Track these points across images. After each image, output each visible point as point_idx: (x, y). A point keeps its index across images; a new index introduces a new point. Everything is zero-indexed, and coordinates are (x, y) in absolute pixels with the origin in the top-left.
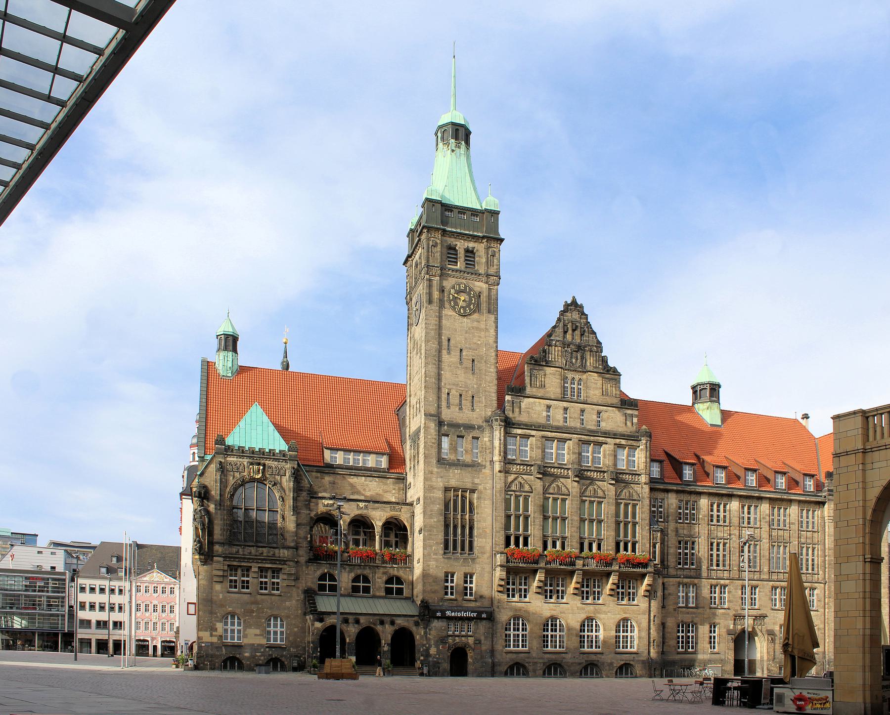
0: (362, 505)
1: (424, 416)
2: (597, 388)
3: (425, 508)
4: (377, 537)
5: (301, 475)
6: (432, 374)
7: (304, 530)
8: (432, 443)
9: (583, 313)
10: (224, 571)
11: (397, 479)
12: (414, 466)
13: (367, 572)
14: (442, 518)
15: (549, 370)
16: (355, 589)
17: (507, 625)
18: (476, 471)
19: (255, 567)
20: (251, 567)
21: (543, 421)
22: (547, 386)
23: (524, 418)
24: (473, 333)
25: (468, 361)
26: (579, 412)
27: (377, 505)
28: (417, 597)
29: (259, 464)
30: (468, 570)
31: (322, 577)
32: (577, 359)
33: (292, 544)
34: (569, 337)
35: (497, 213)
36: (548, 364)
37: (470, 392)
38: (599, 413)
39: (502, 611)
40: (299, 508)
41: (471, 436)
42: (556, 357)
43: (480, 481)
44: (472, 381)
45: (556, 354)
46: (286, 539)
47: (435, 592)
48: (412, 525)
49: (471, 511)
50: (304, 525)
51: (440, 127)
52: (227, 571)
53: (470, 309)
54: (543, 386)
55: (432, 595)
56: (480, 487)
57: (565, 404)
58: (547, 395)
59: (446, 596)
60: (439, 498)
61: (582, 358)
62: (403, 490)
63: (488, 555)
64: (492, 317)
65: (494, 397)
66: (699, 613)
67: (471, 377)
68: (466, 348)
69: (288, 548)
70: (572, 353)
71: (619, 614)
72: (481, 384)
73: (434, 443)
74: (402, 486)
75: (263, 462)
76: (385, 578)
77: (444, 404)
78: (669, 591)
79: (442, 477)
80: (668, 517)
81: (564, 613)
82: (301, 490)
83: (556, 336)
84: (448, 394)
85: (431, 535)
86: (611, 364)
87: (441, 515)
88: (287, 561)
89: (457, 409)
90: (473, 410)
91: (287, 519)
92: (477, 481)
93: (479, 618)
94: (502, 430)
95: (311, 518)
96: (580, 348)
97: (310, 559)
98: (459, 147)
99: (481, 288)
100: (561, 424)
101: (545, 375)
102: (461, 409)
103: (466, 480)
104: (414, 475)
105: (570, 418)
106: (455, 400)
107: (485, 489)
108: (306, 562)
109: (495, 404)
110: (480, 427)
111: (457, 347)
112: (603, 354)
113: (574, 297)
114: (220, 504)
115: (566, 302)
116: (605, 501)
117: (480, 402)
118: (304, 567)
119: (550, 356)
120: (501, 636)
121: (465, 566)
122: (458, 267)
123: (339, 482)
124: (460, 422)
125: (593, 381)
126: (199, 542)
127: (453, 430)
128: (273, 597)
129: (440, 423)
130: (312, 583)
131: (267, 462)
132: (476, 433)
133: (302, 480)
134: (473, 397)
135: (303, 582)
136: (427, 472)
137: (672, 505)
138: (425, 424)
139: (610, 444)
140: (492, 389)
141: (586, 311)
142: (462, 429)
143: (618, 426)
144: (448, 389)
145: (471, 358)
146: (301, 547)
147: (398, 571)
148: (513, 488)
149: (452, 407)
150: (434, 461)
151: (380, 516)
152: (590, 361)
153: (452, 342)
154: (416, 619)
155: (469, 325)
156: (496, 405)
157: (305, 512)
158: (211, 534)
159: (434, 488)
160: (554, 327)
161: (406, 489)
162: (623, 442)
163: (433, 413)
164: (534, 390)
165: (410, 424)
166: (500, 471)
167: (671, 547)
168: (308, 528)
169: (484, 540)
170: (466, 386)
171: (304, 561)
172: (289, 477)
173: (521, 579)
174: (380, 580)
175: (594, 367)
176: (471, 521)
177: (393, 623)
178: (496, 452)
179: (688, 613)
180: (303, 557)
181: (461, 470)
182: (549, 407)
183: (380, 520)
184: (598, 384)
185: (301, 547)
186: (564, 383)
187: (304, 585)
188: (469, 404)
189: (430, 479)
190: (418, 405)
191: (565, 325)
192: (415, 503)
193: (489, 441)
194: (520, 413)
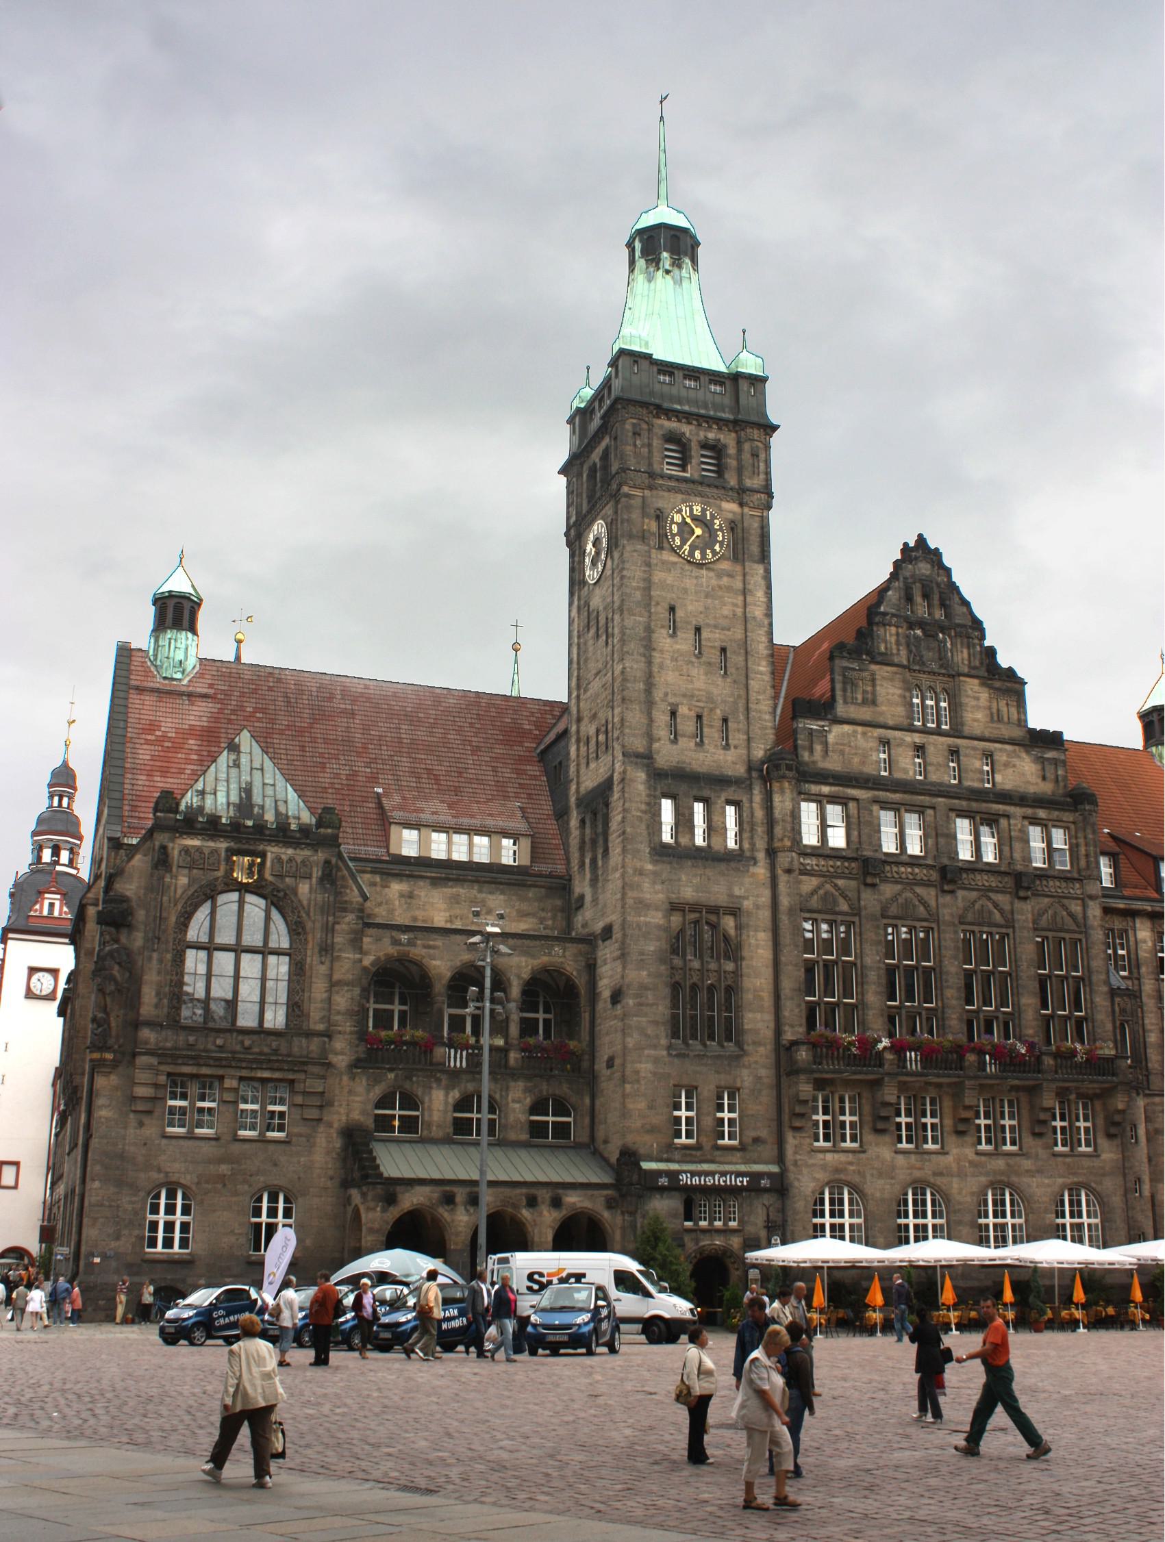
1: (620, 757)
2: (978, 708)
5: (343, 877)
6: (639, 674)
7: (349, 995)
8: (642, 811)
10: (156, 1086)
11: (550, 888)
12: (594, 861)
15: (881, 671)
16: (462, 1127)
17: (815, 1204)
19: (232, 1077)
20: (221, 1078)
22: (880, 699)
23: (833, 764)
24: (722, 597)
28: (606, 1142)
30: (724, 1079)
33: (321, 1027)
35: (763, 380)
37: (718, 711)
40: (337, 947)
41: (723, 799)
44: (723, 689)
46: (309, 1015)
47: (652, 1130)
50: (347, 984)
51: (640, 232)
52: (165, 1086)
53: (714, 553)
55: (647, 1138)
56: (747, 904)
57: (917, 738)
58: (881, 720)
59: (676, 1141)
67: (720, 681)
68: (708, 625)
69: (309, 1034)
73: (645, 812)
80: (1138, 967)
81: (941, 1174)
82: (345, 910)
85: (641, 1004)
86: (1004, 661)
89: (692, 744)
92: (737, 891)
95: (365, 969)
97: (358, 1060)
98: (680, 267)
99: (734, 513)
101: (873, 680)
103: (716, 888)
108: (356, 1064)
111: (688, 623)
113: (920, 536)
114: (159, 939)
115: (906, 544)
118: (345, 1078)
120: (804, 1228)
122: (688, 475)
123: (423, 894)
128: (271, 1147)
130: (363, 1112)
132: (730, 793)
133: (346, 887)
134: (725, 720)
135: (342, 1111)
136: (630, 871)
138: (624, 772)
139: (1015, 818)
143: (1028, 782)
146: (340, 1032)
149: (683, 742)
153: (680, 613)
155: (714, 582)
156: (772, 737)
157: (349, 955)
162: (1042, 814)
163: (641, 750)
165: (578, 777)
168: (357, 991)
170: (710, 699)
172: (321, 880)
173: (842, 1100)
174: (517, 1106)
175: (969, 667)
177: (556, 1203)
180: (342, 1053)
184: (982, 700)
185: (340, 1032)
187: (344, 1118)
189: (638, 887)
190: (602, 738)
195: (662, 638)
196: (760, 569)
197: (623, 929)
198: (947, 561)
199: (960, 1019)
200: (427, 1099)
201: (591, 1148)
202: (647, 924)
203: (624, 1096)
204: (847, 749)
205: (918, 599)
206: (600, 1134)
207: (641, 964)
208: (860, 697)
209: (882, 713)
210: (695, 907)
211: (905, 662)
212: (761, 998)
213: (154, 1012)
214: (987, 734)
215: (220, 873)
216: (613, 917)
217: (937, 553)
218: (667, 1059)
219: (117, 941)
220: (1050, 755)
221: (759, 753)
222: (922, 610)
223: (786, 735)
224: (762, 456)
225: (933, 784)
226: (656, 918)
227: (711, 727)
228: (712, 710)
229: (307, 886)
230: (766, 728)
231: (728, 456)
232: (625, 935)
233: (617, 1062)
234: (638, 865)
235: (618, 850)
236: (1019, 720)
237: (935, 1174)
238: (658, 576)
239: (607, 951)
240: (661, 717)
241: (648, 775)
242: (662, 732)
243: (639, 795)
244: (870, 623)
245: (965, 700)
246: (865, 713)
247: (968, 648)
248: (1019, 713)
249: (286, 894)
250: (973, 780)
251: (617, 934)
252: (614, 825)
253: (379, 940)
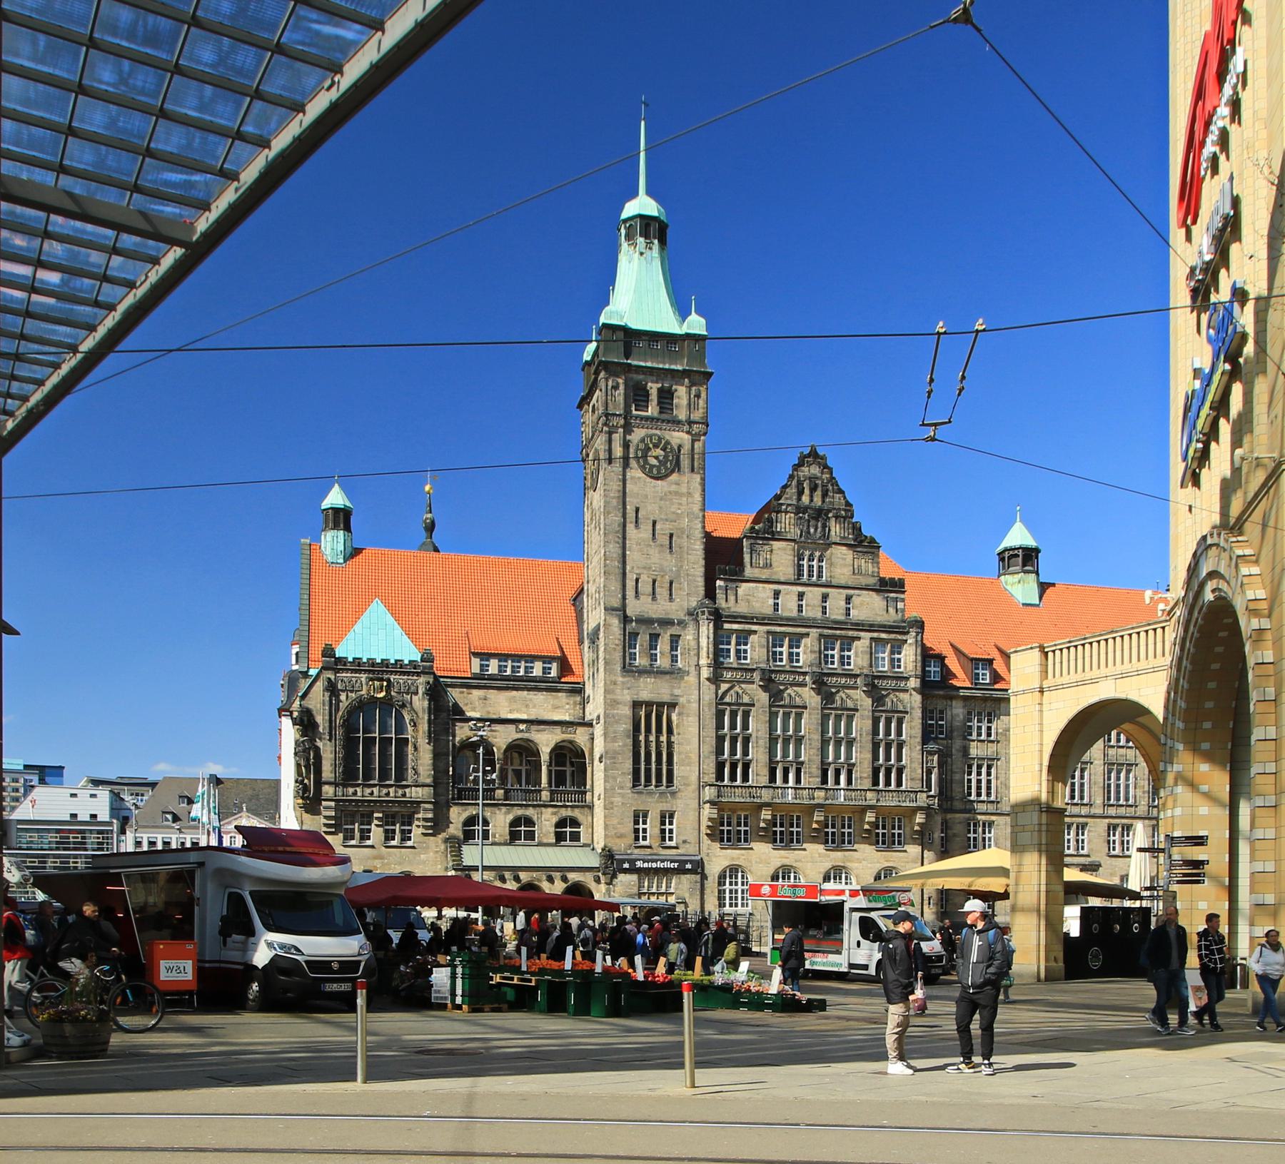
0: (522, 727)
2: (845, 565)
3: (606, 728)
4: (544, 768)
12: (593, 675)
14: (630, 742)
15: (776, 545)
18: (676, 678)
22: (774, 564)
23: (742, 608)
25: (664, 537)
26: (820, 598)
32: (816, 529)
34: (805, 499)
36: (775, 536)
37: (667, 577)
38: (848, 599)
41: (669, 634)
42: (787, 526)
43: (682, 691)
44: (670, 562)
45: (787, 522)
48: (592, 749)
49: (670, 731)
54: (768, 565)
57: (800, 589)
58: (775, 578)
60: (626, 716)
61: (824, 526)
62: (580, 704)
64: (697, 478)
65: (700, 582)
70: (809, 521)
72: (682, 566)
73: (617, 645)
74: (578, 699)
77: (630, 593)
83: (787, 499)
84: (637, 580)
87: (628, 737)
90: (671, 599)
91: (421, 749)
94: (711, 625)
96: (820, 514)
100: (794, 613)
101: (771, 551)
102: (654, 598)
104: (594, 686)
105: (806, 605)
106: (645, 587)
109: (701, 591)
110: (681, 623)
112: (854, 520)
116: (857, 714)
117: (680, 589)
119: (779, 525)
124: (654, 616)
126: (302, 782)
127: (644, 627)
129: (626, 620)
131: (392, 677)
132: (674, 630)
134: (671, 583)
138: (605, 620)
140: (698, 571)
141: (829, 464)
142: (656, 625)
144: (637, 574)
145: (668, 532)
148: (727, 699)
150: (618, 667)
151: (548, 740)
156: (703, 593)
160: (785, 487)
161: (584, 703)
164: (757, 570)
166: (708, 679)
170: (662, 570)
172: (423, 694)
176: (670, 744)
178: (703, 653)
182: (777, 594)
183: (547, 745)
186: (799, 560)
188: (666, 593)
191: (800, 484)
192: (594, 722)
193: (694, 639)
194: (737, 602)
214: (850, 584)
230: (697, 587)
240: (630, 584)
243: (614, 634)
246: (764, 574)
247: (840, 524)
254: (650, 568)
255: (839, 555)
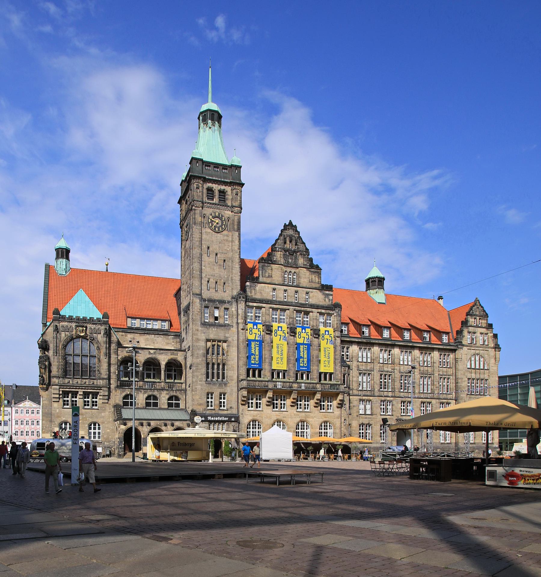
2: (306, 278)
9: (296, 231)
13: (156, 393)
15: (274, 266)
16: (148, 404)
19: (81, 392)
21: (270, 298)
22: (273, 276)
23: (258, 296)
27: (162, 351)
28: (189, 408)
29: (83, 327)
30: (222, 390)
31: (126, 397)
37: (222, 280)
39: (245, 416)
41: (223, 307)
44: (224, 274)
53: (222, 228)
54: (270, 276)
55: (199, 407)
56: (230, 339)
57: (285, 288)
58: (274, 282)
59: (208, 408)
63: (236, 381)
66: (373, 418)
68: (220, 252)
71: (321, 418)
75: (86, 325)
76: (167, 397)
78: (354, 404)
79: (204, 333)
81: (285, 417)
85: (197, 369)
88: (102, 387)
89: (214, 291)
92: (227, 335)
93: (230, 421)
99: (229, 215)
101: (272, 269)
107: (233, 340)
110: (229, 302)
111: (214, 252)
113: (290, 221)
115: (285, 224)
121: (220, 388)
122: (214, 202)
124: (216, 299)
125: (303, 273)
127: (211, 304)
129: (203, 300)
130: (119, 401)
132: (227, 306)
134: (224, 283)
136: (194, 330)
137: (355, 350)
138: (193, 300)
143: (320, 301)
144: (208, 278)
147: (176, 392)
152: (301, 261)
153: (211, 249)
154: (188, 422)
155: (222, 238)
158: (50, 372)
159: (199, 340)
162: (323, 311)
163: (198, 293)
164: (265, 278)
167: (354, 377)
169: (233, 372)
170: (220, 276)
171: (114, 387)
172: (104, 334)
175: (303, 264)
179: (366, 418)
181: (217, 328)
183: (164, 361)
184: (307, 275)
189: (197, 335)
192: (187, 350)
193: (235, 310)
195: (205, 257)
196: (237, 233)
197: (192, 347)
198: (298, 229)
199: (294, 373)
200: (138, 397)
201: (185, 410)
202: (199, 345)
203: (193, 395)
204: (262, 292)
205: (288, 242)
206: (187, 406)
207: (197, 358)
208: (267, 275)
209: (274, 280)
210: (214, 341)
211: (283, 264)
212: (234, 367)
213: (57, 373)
214: (308, 286)
215: (74, 333)
216: (190, 344)
217: (295, 226)
218: (205, 385)
219: (45, 353)
220: (327, 292)
221: (235, 293)
222: (288, 246)
223: (243, 288)
224: (239, 194)
225: (289, 302)
226: (203, 344)
227: (220, 285)
228: (220, 280)
229: (100, 336)
230: (237, 285)
231: (228, 195)
232: (193, 349)
233: (191, 385)
234: (197, 328)
235: (191, 324)
236: (318, 281)
237: (283, 417)
238: (204, 236)
239: (189, 354)
240: (204, 282)
241: (200, 301)
242: (204, 287)
243: (197, 307)
244: (272, 251)
245: (301, 275)
246: (268, 280)
247: (304, 258)
248: (319, 279)
249: (94, 339)
250: (302, 301)
251: (191, 349)
252: (190, 316)
253: (122, 351)
254: (214, 276)
255: (303, 273)
